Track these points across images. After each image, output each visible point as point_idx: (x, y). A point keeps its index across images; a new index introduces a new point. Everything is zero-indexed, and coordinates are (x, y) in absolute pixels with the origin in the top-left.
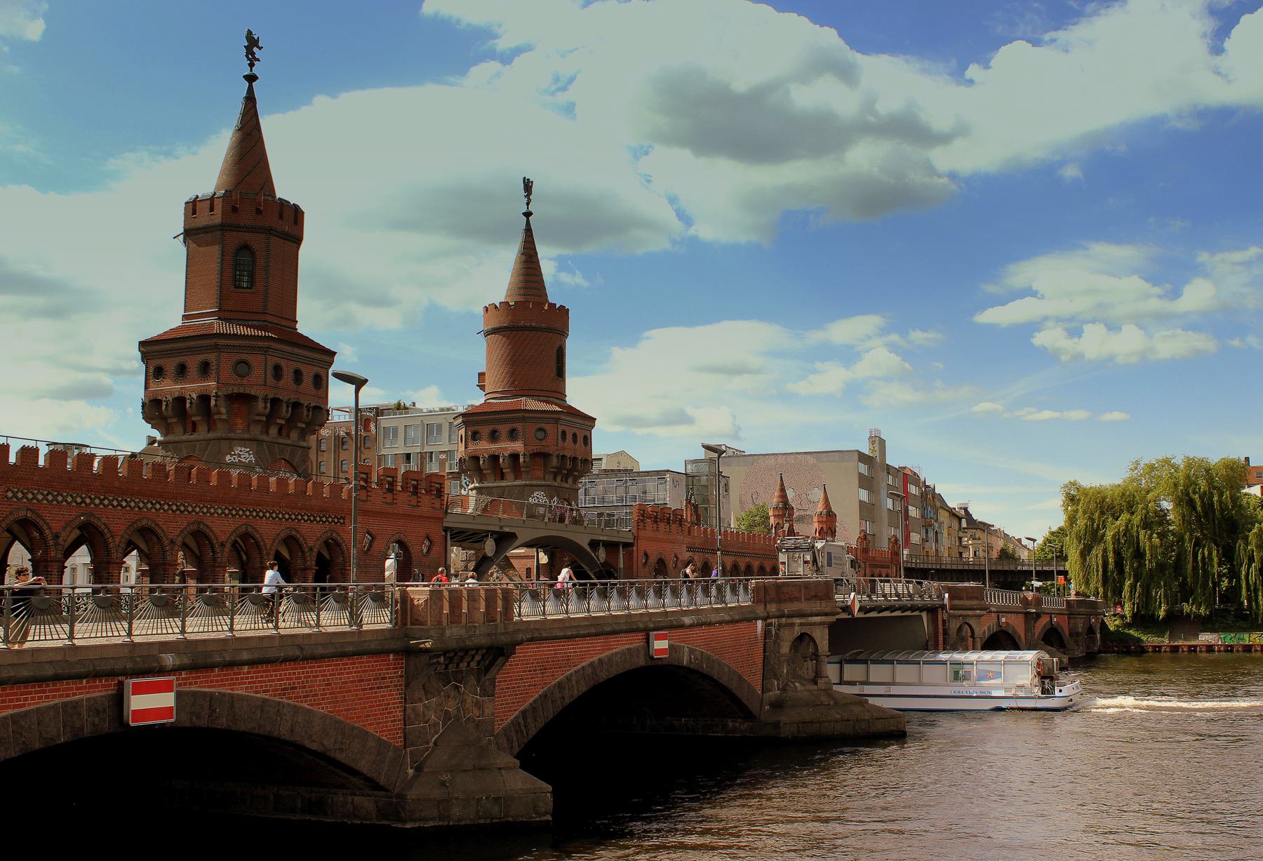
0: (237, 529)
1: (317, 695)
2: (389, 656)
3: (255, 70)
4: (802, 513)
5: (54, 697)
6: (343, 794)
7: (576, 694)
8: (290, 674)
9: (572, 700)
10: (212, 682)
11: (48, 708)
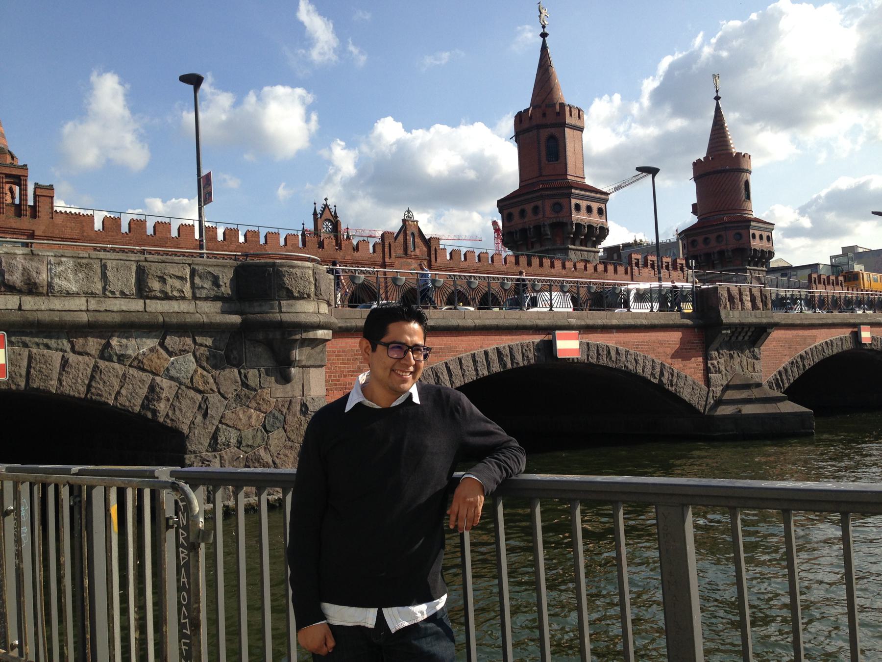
9: (810, 367)
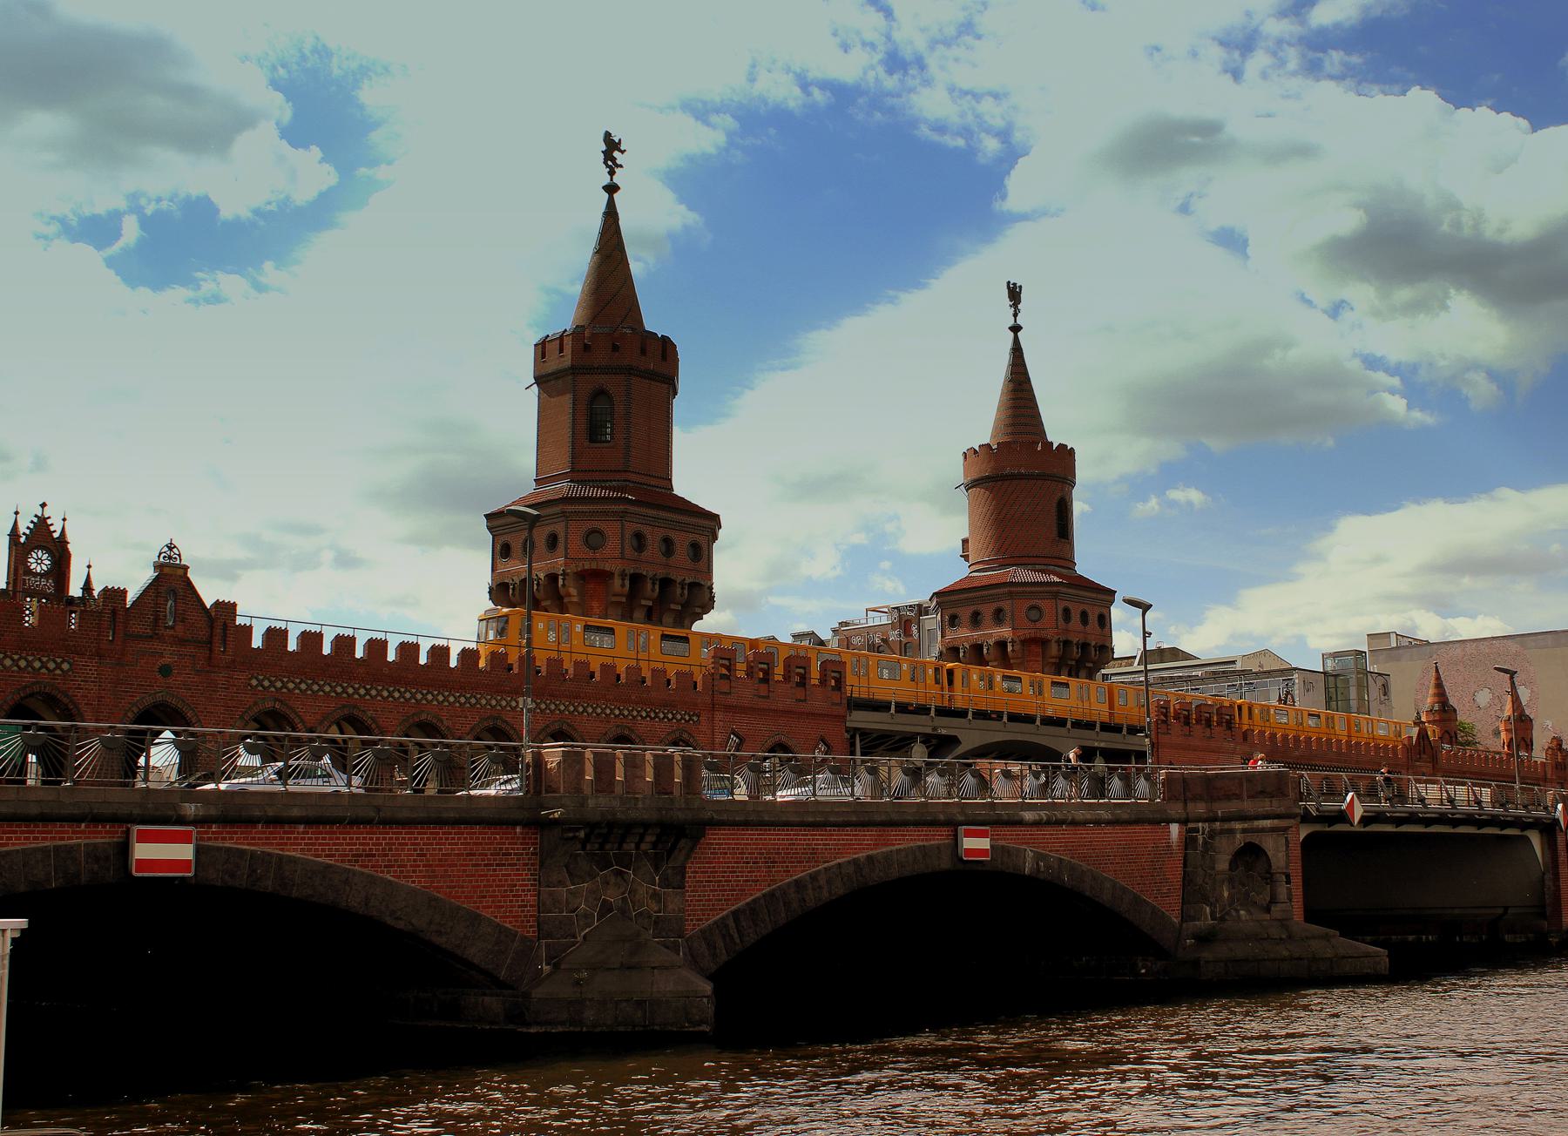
0: (548, 726)
1: (405, 866)
2: (515, 829)
3: (616, 179)
5: (44, 839)
10: (254, 838)
11: (35, 850)
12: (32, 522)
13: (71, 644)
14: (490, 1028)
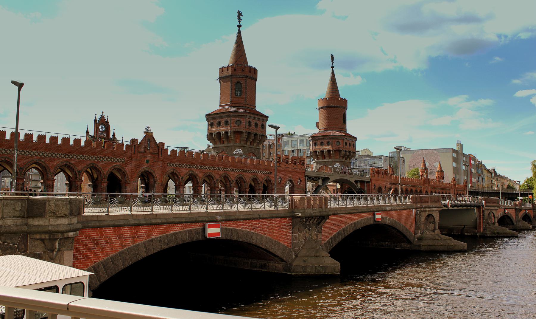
1: (264, 230)
4: (431, 171)
5: (185, 228)
6: (272, 263)
7: (349, 233)
8: (255, 223)
10: (232, 225)
11: (184, 231)
12: (100, 117)
13: (125, 154)
14: (278, 272)
